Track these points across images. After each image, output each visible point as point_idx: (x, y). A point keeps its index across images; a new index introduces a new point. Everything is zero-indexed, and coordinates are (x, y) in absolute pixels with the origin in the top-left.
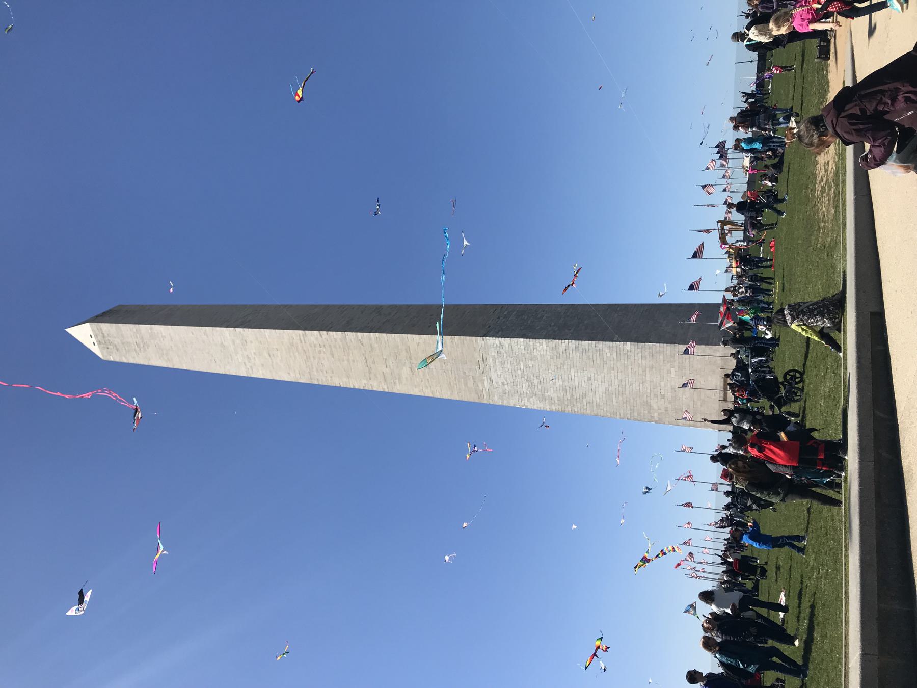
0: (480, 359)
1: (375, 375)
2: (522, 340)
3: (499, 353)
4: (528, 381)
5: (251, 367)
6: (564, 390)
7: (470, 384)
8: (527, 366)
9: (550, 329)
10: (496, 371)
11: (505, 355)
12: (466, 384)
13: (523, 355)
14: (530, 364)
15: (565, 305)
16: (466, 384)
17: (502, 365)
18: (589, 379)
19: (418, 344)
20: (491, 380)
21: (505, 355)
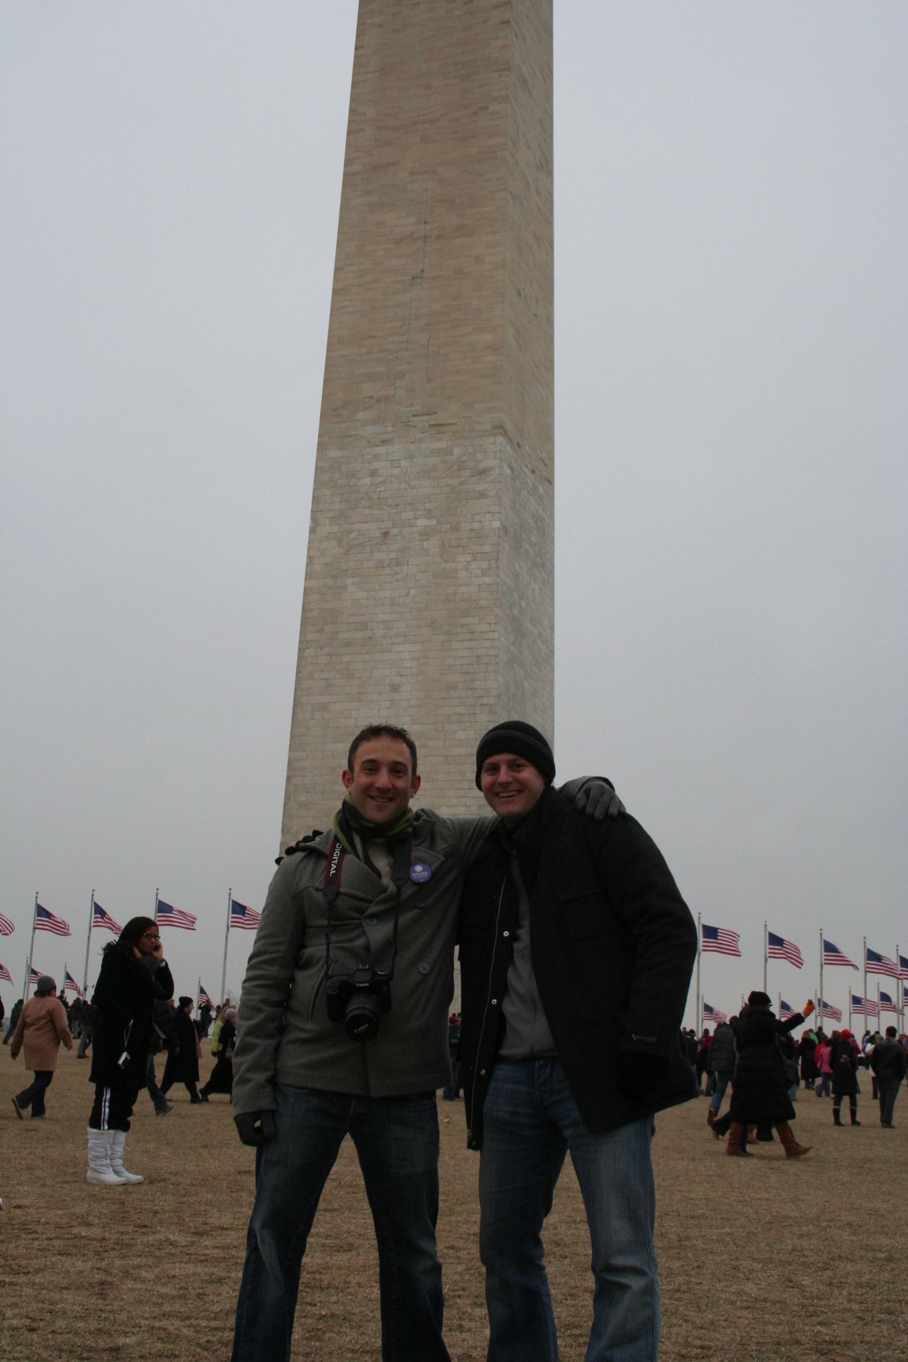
2: (496, 524)
6: (363, 626)
8: (425, 534)
9: (515, 595)
10: (411, 457)
11: (454, 482)
13: (456, 528)
14: (433, 544)
15: (553, 639)
18: (395, 688)
20: (384, 442)
21: (454, 482)
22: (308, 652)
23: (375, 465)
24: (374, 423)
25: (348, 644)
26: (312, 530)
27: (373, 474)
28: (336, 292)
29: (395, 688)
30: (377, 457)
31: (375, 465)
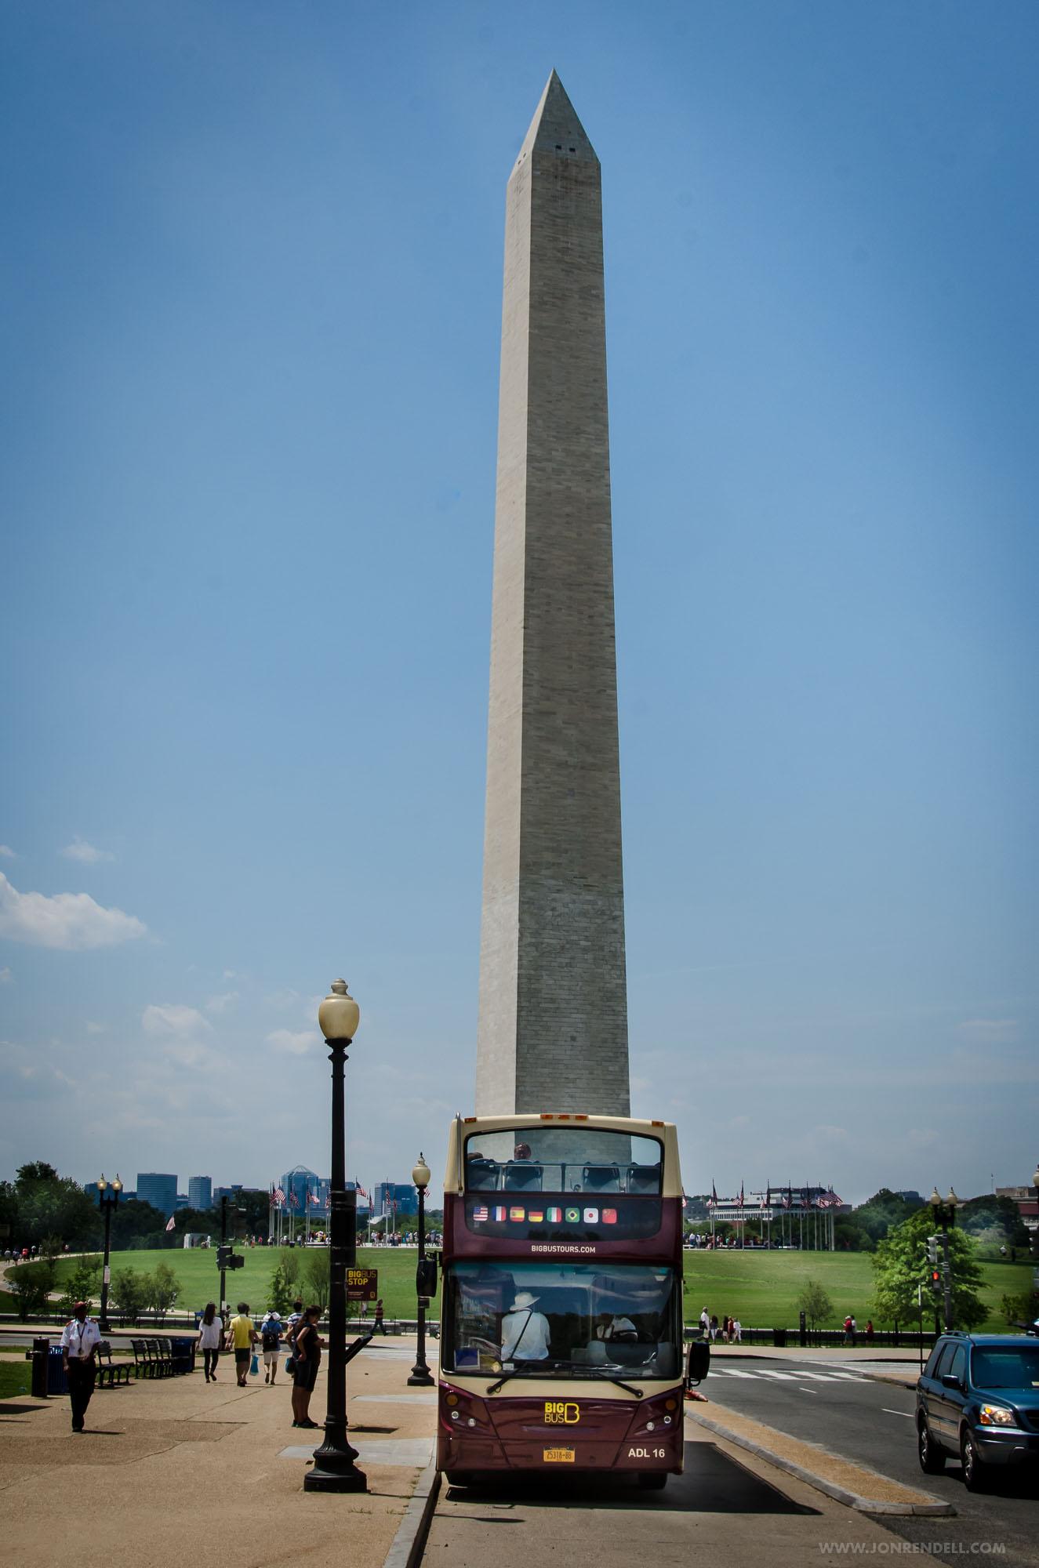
0: (590, 881)
1: (548, 699)
3: (603, 913)
4: (563, 948)
5: (543, 470)
6: (552, 1001)
7: (548, 857)
8: (585, 950)
10: (574, 902)
12: (547, 849)
13: (602, 948)
14: (589, 956)
16: (547, 849)
17: (584, 914)
18: (573, 1039)
19: (605, 787)
20: (559, 891)
22: (523, 1013)
23: (554, 904)
24: (552, 878)
25: (545, 1010)
26: (520, 939)
27: (553, 909)
28: (523, 790)
29: (573, 1039)
30: (554, 900)
31: (554, 904)
